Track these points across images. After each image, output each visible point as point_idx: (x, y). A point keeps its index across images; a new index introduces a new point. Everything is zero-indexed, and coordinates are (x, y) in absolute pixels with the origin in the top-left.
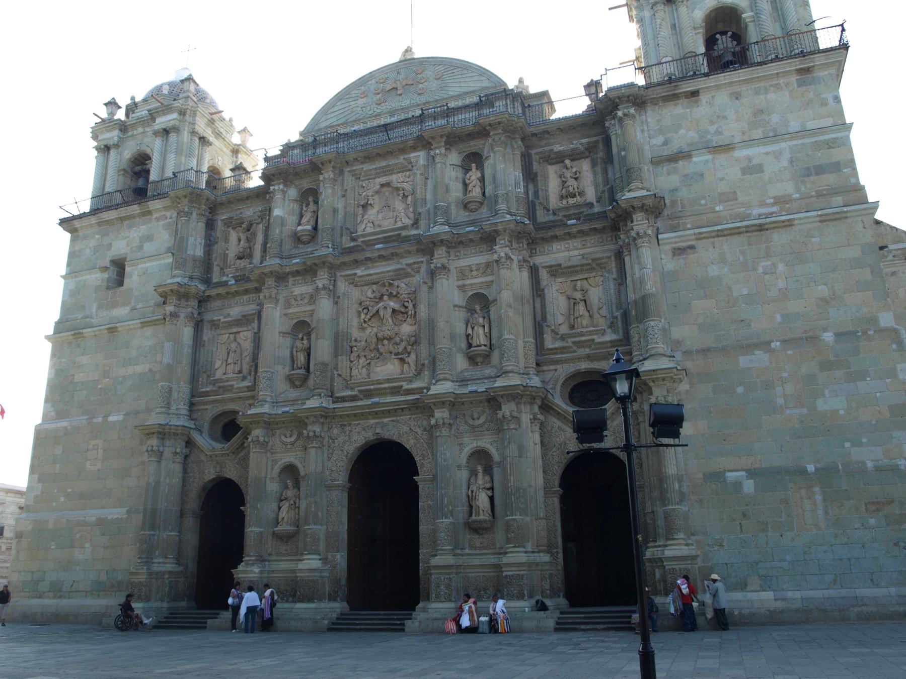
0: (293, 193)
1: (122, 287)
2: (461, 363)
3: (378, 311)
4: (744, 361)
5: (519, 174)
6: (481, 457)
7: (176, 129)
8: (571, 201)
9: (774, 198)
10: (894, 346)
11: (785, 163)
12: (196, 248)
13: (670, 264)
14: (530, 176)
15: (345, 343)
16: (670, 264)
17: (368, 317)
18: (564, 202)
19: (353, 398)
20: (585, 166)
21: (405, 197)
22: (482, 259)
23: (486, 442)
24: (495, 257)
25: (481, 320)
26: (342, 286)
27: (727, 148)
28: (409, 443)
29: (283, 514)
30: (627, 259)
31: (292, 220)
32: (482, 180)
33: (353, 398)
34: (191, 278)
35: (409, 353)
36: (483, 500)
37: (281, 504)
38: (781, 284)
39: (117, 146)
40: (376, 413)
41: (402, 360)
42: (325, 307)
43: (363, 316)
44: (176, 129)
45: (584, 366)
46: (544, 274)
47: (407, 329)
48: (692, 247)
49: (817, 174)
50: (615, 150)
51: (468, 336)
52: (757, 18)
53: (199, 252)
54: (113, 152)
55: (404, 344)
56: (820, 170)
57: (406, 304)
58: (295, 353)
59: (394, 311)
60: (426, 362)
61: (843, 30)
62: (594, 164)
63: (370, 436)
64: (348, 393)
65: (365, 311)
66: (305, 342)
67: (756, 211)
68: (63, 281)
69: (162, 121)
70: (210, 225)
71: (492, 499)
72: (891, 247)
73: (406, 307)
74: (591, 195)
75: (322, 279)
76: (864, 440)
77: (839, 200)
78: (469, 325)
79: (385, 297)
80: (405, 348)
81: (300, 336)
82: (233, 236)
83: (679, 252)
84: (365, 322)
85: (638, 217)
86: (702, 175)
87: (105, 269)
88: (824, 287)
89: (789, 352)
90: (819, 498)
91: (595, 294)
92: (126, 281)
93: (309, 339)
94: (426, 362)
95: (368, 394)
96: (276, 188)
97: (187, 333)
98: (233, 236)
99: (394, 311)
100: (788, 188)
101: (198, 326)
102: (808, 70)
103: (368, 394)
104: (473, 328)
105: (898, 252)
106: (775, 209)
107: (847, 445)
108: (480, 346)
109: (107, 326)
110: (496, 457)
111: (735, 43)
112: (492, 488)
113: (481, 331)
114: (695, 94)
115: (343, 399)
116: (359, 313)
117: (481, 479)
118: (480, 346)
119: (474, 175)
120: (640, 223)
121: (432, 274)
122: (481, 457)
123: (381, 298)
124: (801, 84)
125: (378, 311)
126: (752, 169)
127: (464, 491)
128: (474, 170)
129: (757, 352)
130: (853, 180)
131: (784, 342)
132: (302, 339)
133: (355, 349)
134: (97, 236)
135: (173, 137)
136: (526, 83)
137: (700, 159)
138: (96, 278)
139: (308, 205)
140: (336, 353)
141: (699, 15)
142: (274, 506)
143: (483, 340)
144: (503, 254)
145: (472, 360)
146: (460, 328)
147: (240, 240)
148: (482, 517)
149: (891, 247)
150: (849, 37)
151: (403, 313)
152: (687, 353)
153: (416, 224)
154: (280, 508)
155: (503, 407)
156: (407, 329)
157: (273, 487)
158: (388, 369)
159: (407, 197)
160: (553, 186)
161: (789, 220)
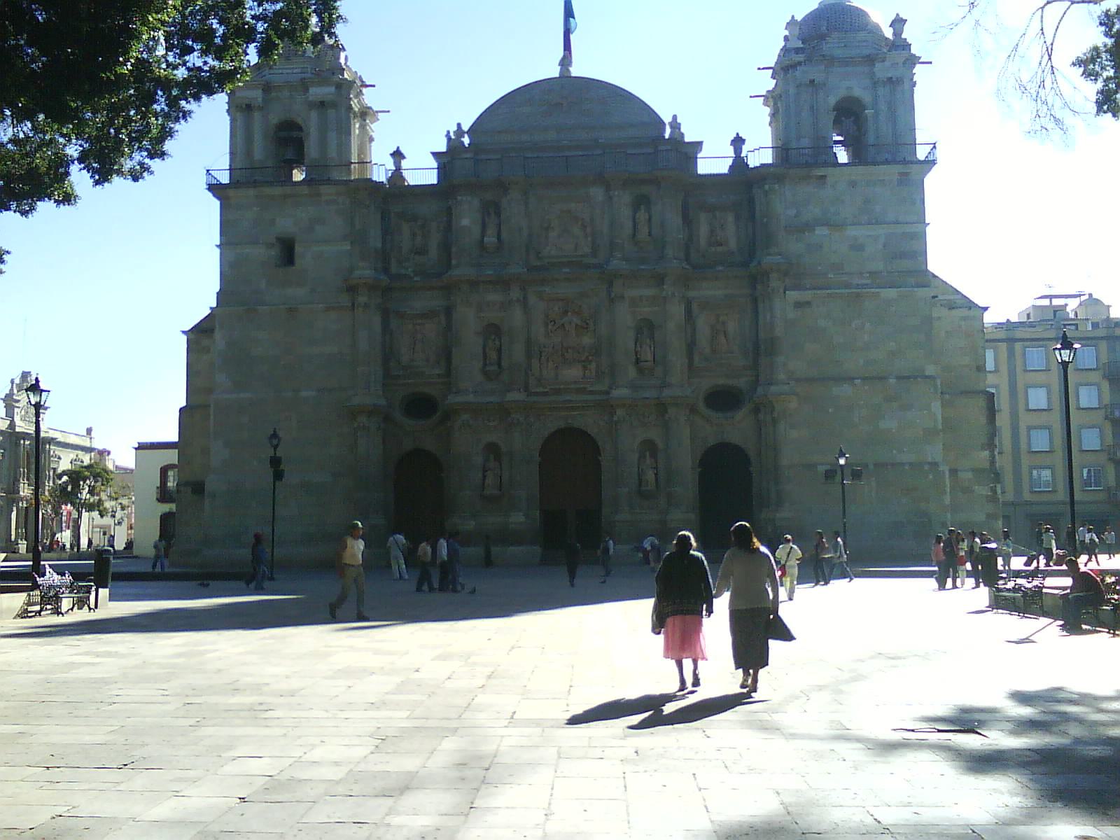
0: (476, 203)
1: (294, 268)
2: (632, 372)
3: (563, 325)
4: (836, 390)
5: (680, 221)
6: (649, 447)
7: (334, 105)
8: (720, 249)
9: (870, 273)
10: (932, 390)
11: (881, 247)
12: (375, 241)
13: (791, 314)
14: (688, 221)
15: (536, 349)
16: (791, 314)
17: (555, 328)
18: (713, 249)
19: (545, 394)
20: (730, 218)
21: (584, 227)
22: (649, 292)
23: (654, 434)
24: (664, 294)
25: (648, 341)
26: (532, 299)
27: (838, 226)
28: (593, 431)
29: (489, 481)
30: (761, 306)
31: (476, 230)
32: (650, 219)
33: (545, 394)
34: (375, 269)
35: (591, 361)
36: (650, 476)
37: (486, 474)
38: (866, 337)
39: (261, 109)
40: (567, 408)
41: (585, 368)
42: (517, 316)
43: (550, 327)
44: (334, 105)
45: (721, 381)
46: (695, 306)
47: (587, 340)
48: (808, 303)
49: (901, 258)
50: (758, 214)
51: (636, 353)
52: (876, 114)
53: (379, 245)
54: (257, 115)
55: (586, 354)
56: (903, 255)
57: (588, 321)
58: (487, 350)
59: (577, 325)
60: (607, 371)
61: (935, 147)
62: (737, 218)
63: (562, 424)
64: (540, 390)
65: (553, 323)
66: (497, 343)
67: (856, 281)
68: (218, 251)
69: (316, 92)
70: (385, 217)
71: (656, 474)
72: (940, 297)
73: (587, 324)
74: (733, 244)
75: (515, 293)
76: (905, 450)
77: (912, 280)
78: (638, 346)
79: (569, 313)
80: (587, 357)
81: (493, 337)
82: (406, 229)
83: (799, 305)
84: (551, 332)
85: (774, 275)
86: (821, 247)
87: (270, 246)
88: (894, 344)
89: (866, 388)
90: (873, 484)
91: (732, 326)
92: (298, 261)
93: (500, 339)
94: (607, 371)
95: (558, 392)
96: (464, 199)
97: (377, 320)
98: (406, 229)
99: (577, 325)
100: (879, 266)
101: (386, 314)
102: (906, 174)
103: (558, 392)
104: (641, 347)
105: (945, 302)
106: (868, 282)
107: (894, 452)
108: (646, 361)
109: (287, 306)
110: (661, 446)
111: (855, 128)
112: (656, 468)
113: (648, 349)
114: (823, 177)
115: (537, 394)
116: (546, 325)
117: (649, 461)
118: (646, 361)
119: (642, 215)
120: (775, 283)
121: (612, 301)
122: (649, 447)
123: (566, 312)
124: (900, 183)
125: (563, 325)
126: (858, 247)
127: (637, 469)
128: (643, 211)
129: (844, 385)
130: (924, 267)
131: (864, 379)
132: (494, 340)
133: (543, 354)
134: (255, 209)
135: (331, 113)
136: (678, 121)
137: (821, 231)
138: (261, 253)
139: (489, 214)
140: (529, 355)
141: (832, 100)
142: (480, 475)
143: (649, 357)
144: (670, 293)
145: (641, 371)
146: (631, 345)
147: (414, 235)
148: (649, 488)
149: (940, 297)
150: (939, 154)
151: (584, 328)
152: (798, 380)
153: (594, 253)
154: (484, 477)
155: (669, 411)
156: (587, 340)
157: (479, 460)
158: (572, 373)
159: (585, 227)
160: (703, 230)
161: (878, 292)
